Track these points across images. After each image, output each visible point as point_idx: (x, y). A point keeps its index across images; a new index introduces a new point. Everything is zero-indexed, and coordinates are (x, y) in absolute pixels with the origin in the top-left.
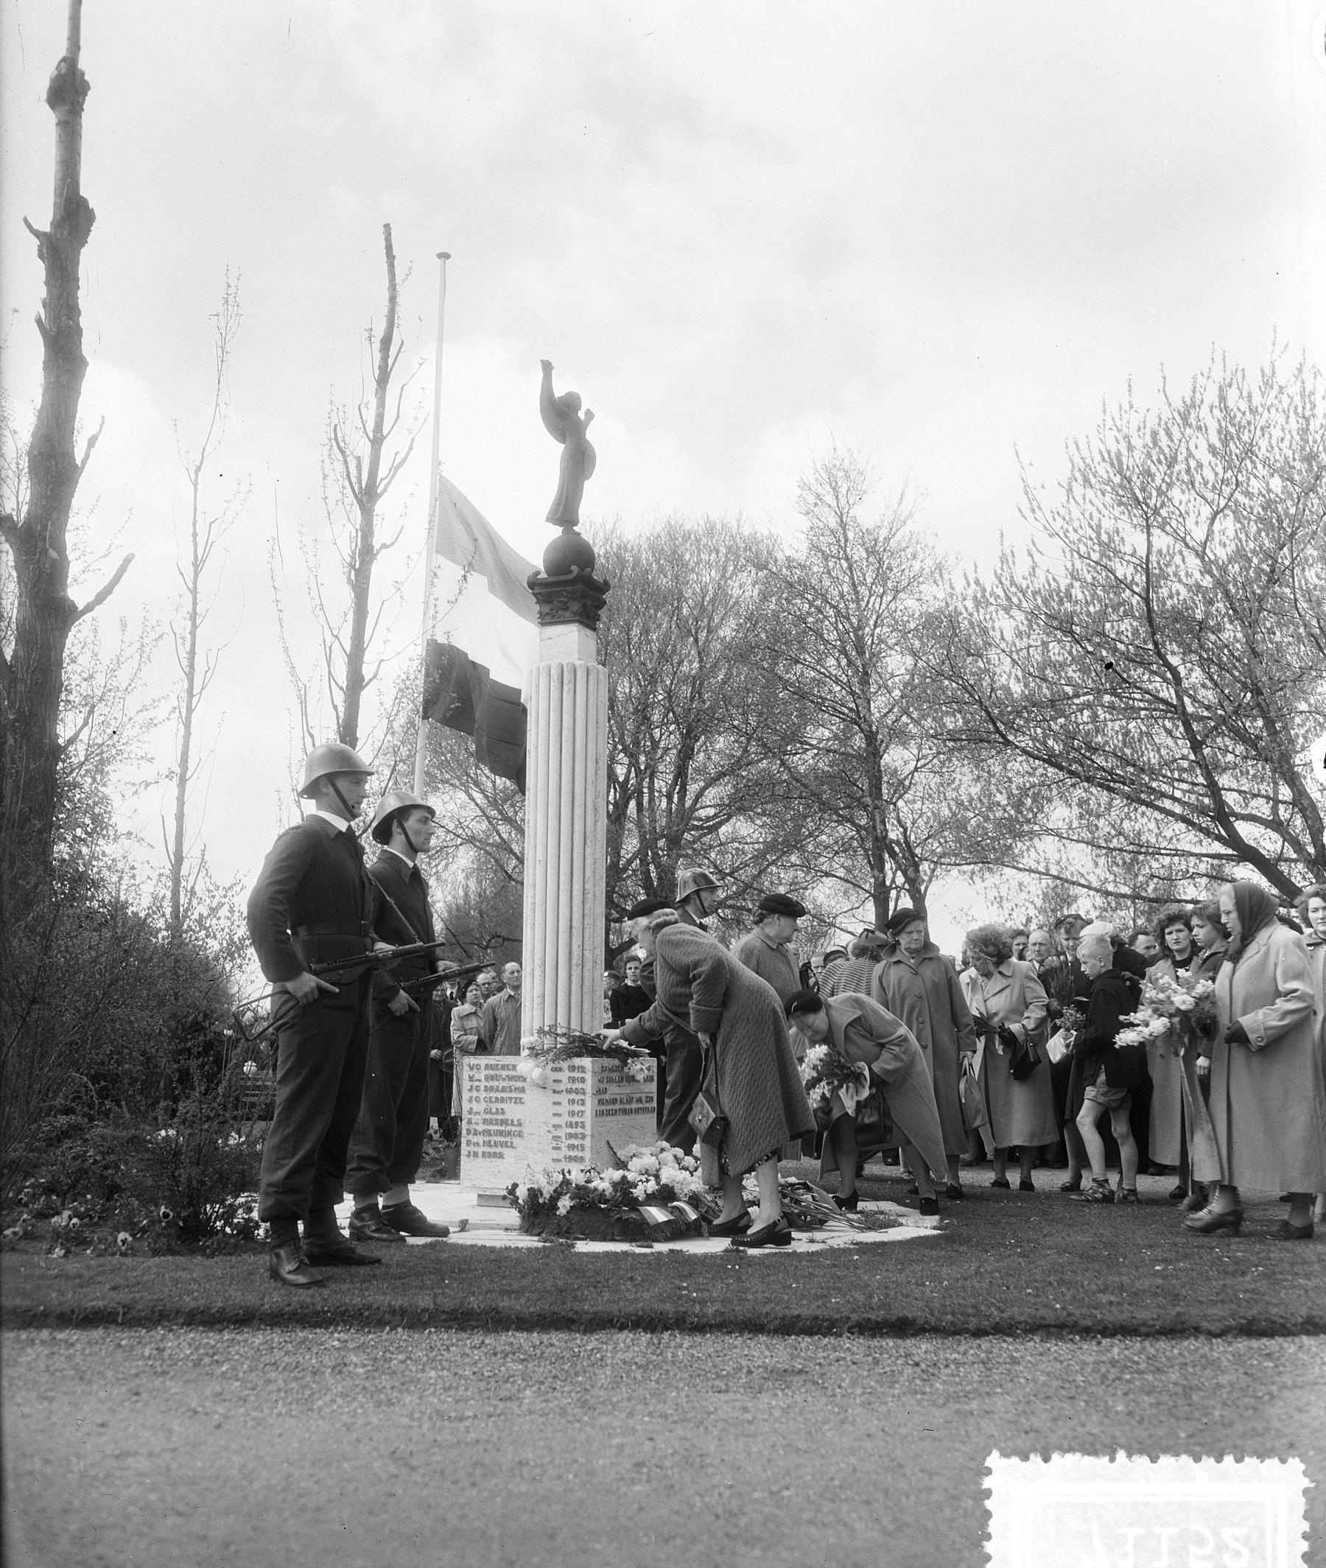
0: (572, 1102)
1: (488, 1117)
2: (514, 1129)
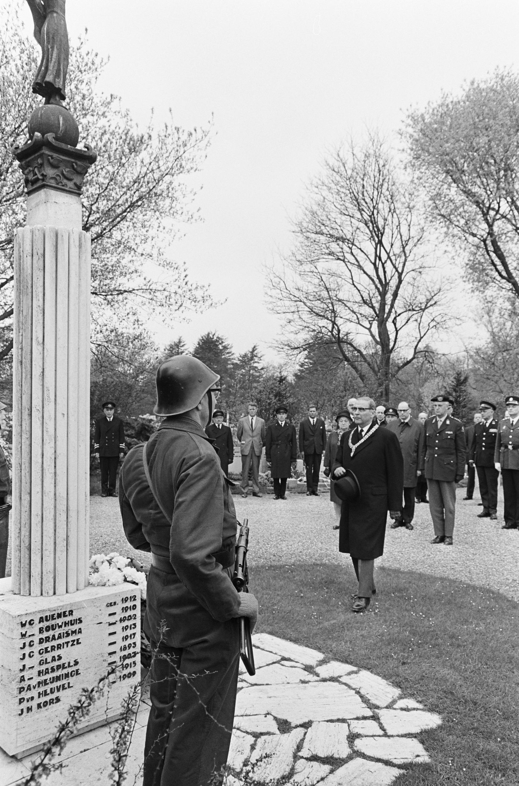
0: (125, 628)
1: (44, 667)
2: (70, 670)
